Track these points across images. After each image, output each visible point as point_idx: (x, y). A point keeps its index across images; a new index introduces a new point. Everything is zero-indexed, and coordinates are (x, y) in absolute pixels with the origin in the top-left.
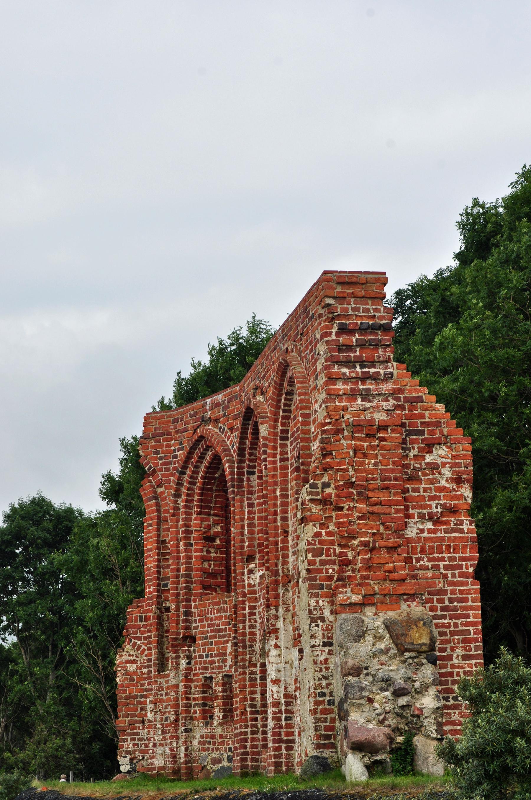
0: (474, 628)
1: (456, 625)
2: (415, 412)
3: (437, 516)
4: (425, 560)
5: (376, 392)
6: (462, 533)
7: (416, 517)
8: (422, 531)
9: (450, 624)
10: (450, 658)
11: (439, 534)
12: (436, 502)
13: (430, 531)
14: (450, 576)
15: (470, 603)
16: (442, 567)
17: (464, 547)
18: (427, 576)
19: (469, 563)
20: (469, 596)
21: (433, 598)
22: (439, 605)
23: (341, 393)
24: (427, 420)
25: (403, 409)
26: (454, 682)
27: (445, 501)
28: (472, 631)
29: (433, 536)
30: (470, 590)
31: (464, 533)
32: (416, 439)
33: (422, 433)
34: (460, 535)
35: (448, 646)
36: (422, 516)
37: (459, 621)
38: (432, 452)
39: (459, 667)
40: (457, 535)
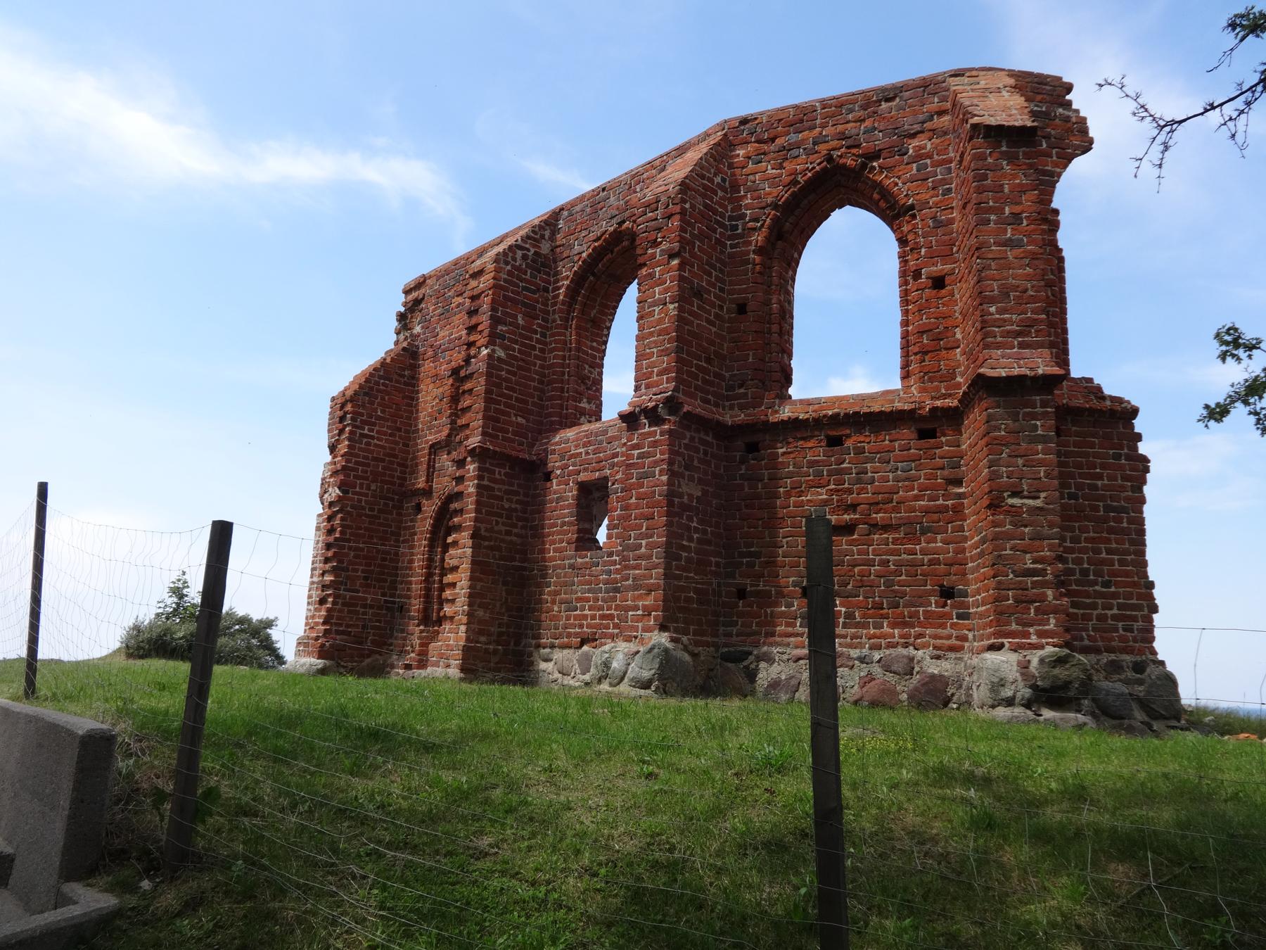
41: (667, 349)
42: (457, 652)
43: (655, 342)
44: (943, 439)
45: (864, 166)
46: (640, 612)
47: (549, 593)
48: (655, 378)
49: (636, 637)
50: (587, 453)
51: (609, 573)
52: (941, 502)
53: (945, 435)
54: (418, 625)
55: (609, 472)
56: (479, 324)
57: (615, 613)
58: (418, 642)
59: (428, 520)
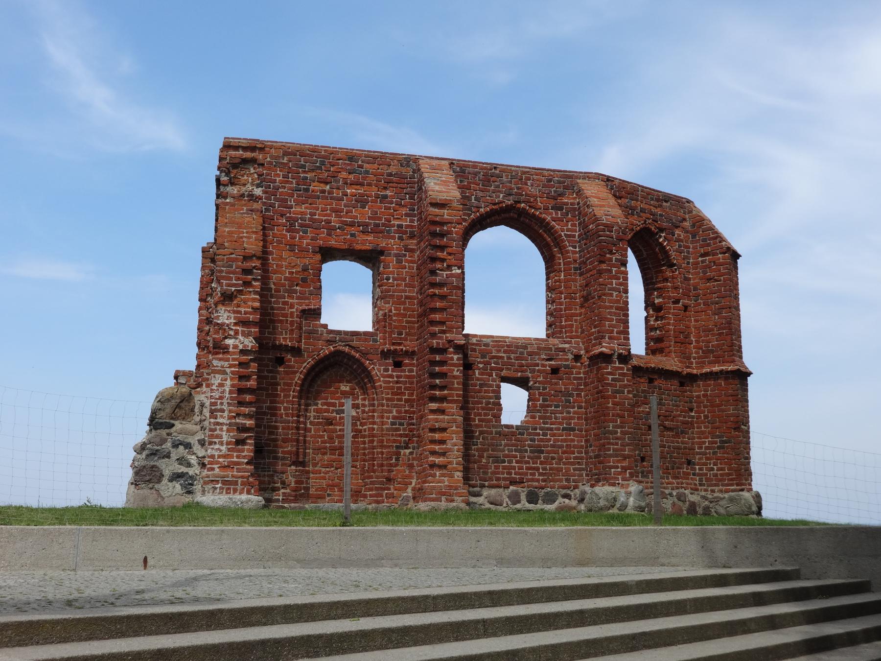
41: (623, 319)
42: (464, 491)
43: (614, 313)
44: (688, 388)
45: (657, 233)
46: (619, 470)
47: (477, 450)
48: (615, 335)
49: (619, 484)
50: (509, 358)
51: (533, 440)
52: (687, 419)
53: (688, 386)
54: (290, 466)
55: (530, 375)
57: (540, 466)
58: (293, 480)
59: (298, 375)
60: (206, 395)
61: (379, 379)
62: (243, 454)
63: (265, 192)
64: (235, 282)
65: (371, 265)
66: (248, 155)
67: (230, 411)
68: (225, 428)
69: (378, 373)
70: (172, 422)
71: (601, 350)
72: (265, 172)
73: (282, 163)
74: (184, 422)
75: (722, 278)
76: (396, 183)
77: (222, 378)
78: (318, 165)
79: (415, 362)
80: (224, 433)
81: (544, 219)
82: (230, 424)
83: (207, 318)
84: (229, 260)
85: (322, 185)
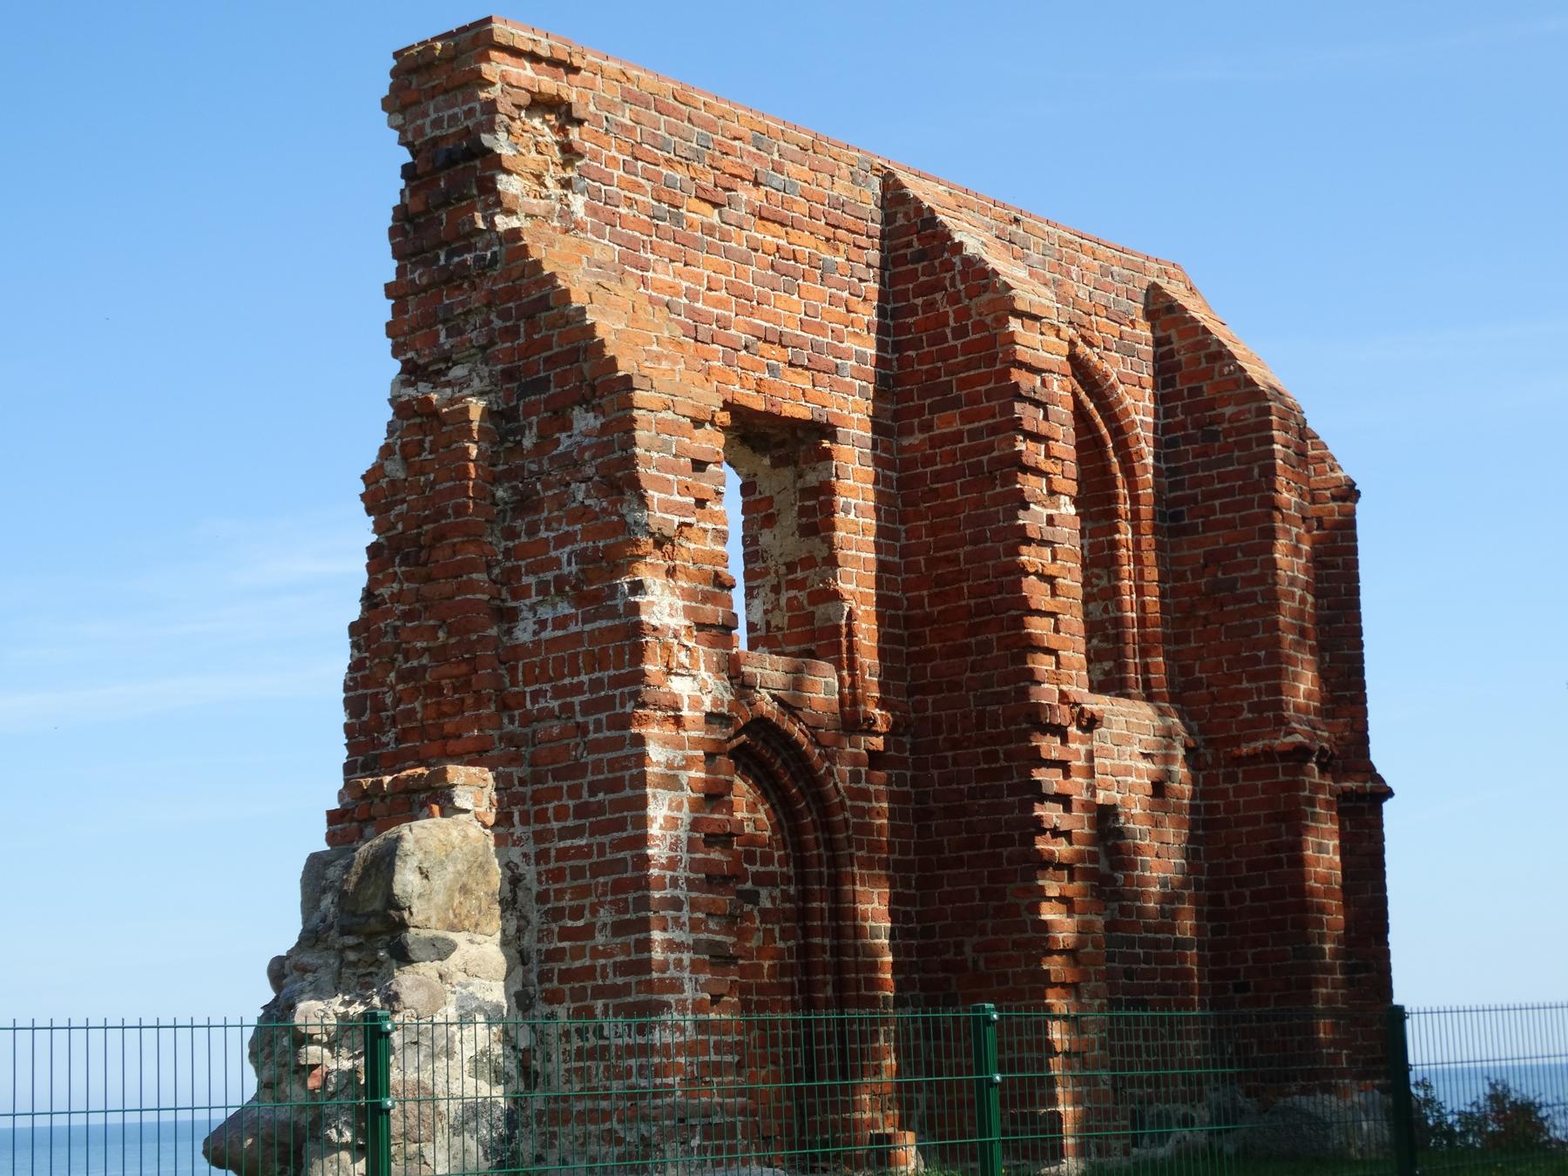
0: (635, 852)
1: (601, 846)
2: (536, 337)
3: (569, 583)
4: (549, 695)
5: (460, 310)
6: (613, 618)
7: (533, 593)
8: (542, 624)
9: (589, 846)
10: (588, 932)
11: (573, 628)
12: (568, 549)
13: (561, 623)
14: (591, 728)
15: (628, 792)
16: (577, 708)
17: (619, 652)
18: (551, 735)
19: (626, 690)
20: (627, 774)
21: (562, 788)
22: (571, 803)
23: (406, 328)
24: (556, 350)
25: (511, 333)
26: (599, 992)
27: (583, 545)
28: (630, 863)
29: (560, 633)
30: (627, 757)
31: (620, 616)
32: (533, 404)
33: (541, 385)
34: (610, 623)
35: (587, 902)
36: (543, 588)
37: (605, 839)
38: (570, 428)
39: (606, 954)
40: (603, 623)
56: (1053, 439)
60: (525, 849)
61: (842, 803)
62: (728, 1039)
63: (592, 211)
64: (678, 498)
65: (767, 461)
66: (548, 83)
67: (694, 906)
68: (686, 957)
69: (840, 785)
70: (452, 936)
71: (1289, 739)
72: (587, 144)
73: (623, 126)
74: (479, 938)
75: (1340, 560)
76: (848, 230)
77: (671, 801)
78: (694, 145)
79: (907, 754)
80: (686, 974)
81: (1106, 376)
82: (696, 947)
83: (492, 598)
84: (663, 427)
85: (707, 207)
